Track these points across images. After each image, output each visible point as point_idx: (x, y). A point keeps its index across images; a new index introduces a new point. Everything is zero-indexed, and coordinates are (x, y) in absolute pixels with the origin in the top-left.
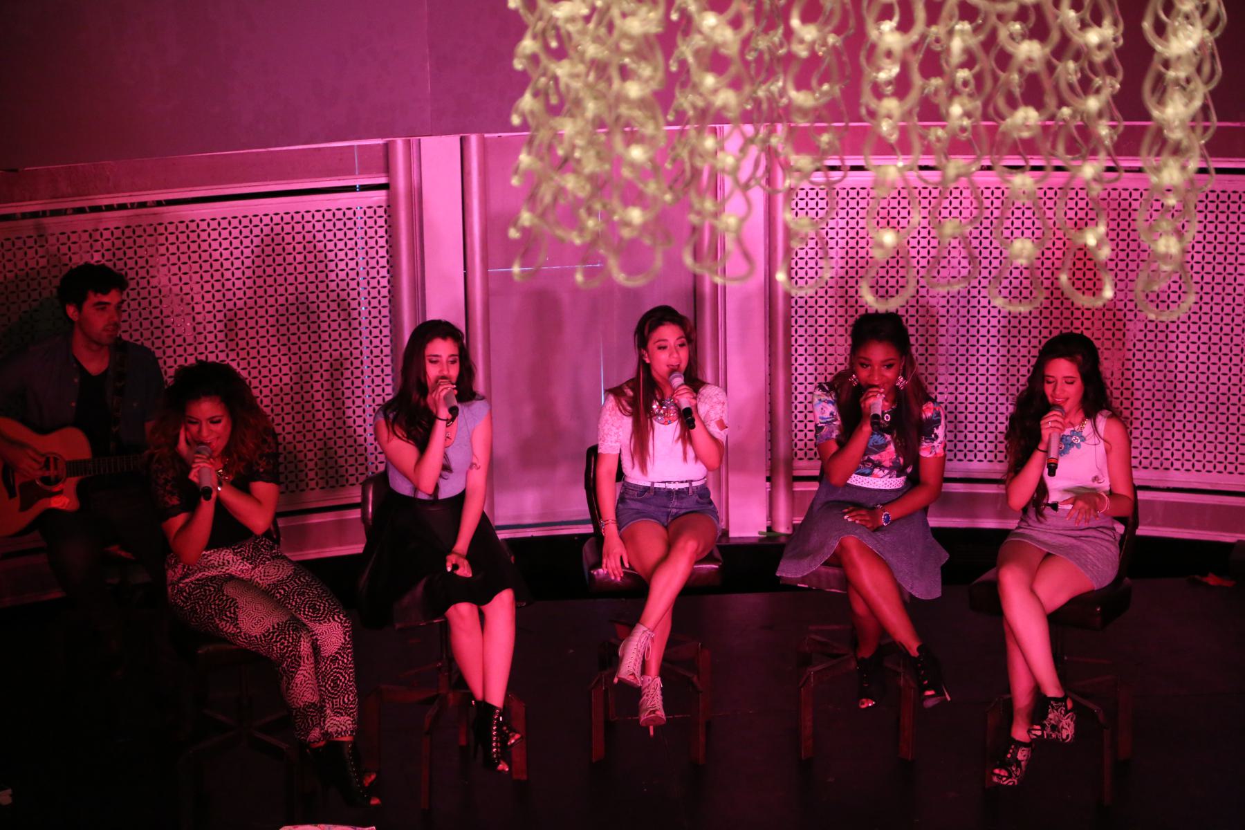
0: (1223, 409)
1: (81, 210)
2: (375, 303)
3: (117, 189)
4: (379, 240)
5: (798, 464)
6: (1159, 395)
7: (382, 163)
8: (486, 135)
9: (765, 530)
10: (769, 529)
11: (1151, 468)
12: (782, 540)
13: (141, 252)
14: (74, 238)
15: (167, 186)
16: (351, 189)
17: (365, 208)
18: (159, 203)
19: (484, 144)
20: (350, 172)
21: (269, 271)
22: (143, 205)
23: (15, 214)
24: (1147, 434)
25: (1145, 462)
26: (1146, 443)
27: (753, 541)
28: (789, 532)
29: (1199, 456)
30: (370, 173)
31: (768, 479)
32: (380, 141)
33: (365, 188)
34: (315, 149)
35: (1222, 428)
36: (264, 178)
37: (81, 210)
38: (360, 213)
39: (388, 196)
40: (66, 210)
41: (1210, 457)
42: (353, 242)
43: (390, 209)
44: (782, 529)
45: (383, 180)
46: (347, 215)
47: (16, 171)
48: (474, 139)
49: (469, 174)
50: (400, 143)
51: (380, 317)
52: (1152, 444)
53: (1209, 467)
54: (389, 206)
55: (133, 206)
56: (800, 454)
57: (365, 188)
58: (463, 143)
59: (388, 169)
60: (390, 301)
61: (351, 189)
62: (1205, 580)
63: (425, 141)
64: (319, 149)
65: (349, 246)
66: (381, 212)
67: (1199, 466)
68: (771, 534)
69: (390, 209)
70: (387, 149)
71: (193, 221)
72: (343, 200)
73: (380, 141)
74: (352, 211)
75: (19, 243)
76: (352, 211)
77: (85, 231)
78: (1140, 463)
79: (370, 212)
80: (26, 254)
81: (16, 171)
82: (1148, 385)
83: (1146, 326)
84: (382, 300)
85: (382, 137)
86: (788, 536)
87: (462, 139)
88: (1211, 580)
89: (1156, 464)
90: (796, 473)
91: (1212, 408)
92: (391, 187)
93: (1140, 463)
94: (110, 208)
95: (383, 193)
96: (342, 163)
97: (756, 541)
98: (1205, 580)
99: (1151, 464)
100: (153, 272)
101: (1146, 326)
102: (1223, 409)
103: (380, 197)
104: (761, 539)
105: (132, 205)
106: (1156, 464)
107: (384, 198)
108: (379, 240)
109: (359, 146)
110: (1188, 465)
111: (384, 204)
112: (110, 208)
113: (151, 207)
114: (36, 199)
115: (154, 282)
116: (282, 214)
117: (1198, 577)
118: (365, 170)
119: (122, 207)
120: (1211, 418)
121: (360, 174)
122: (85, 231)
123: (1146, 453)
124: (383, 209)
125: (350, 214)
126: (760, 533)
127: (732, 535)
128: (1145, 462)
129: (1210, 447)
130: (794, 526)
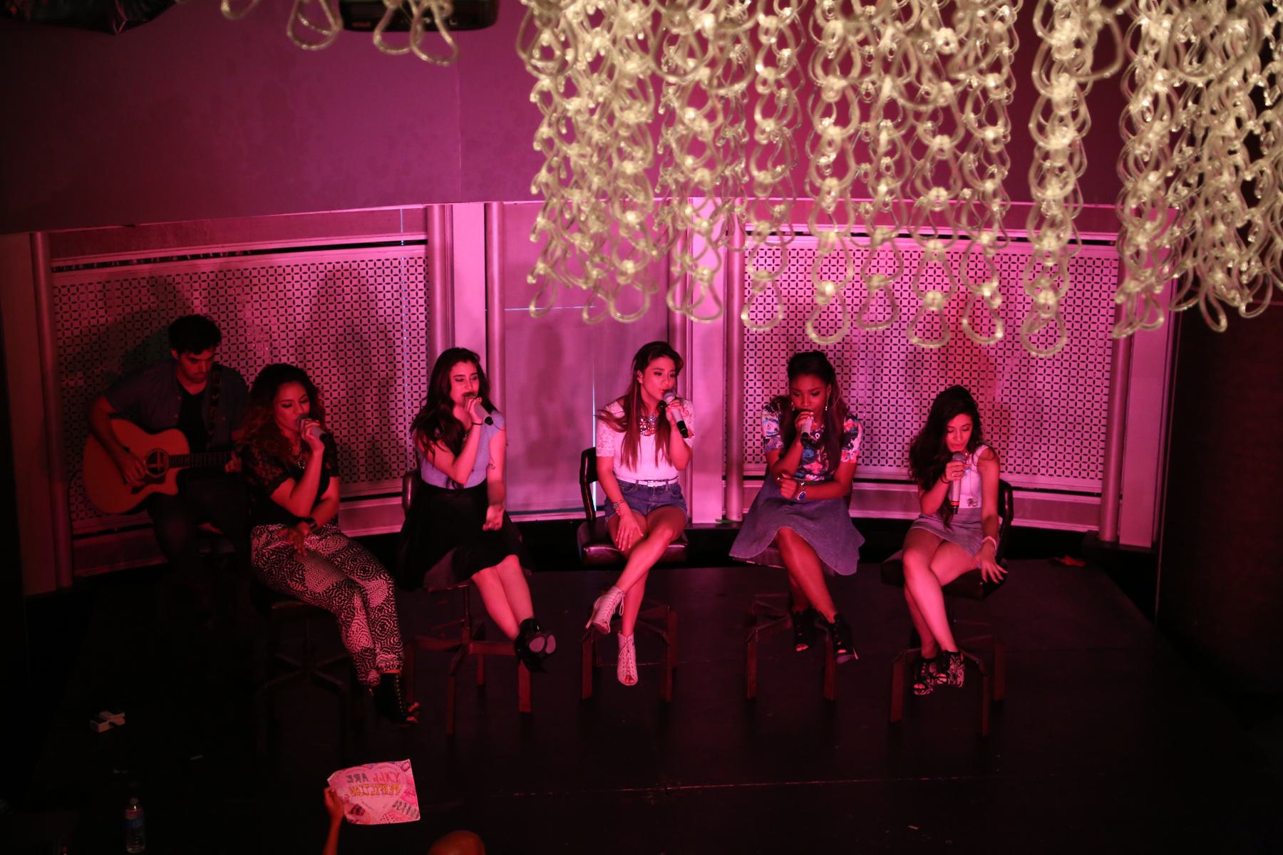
0: (1079, 427)
1: (184, 258)
2: (414, 334)
3: (212, 241)
5: (747, 466)
6: (1030, 416)
8: (505, 203)
9: (721, 518)
10: (724, 517)
11: (1023, 473)
12: (735, 526)
13: (231, 291)
16: (397, 243)
17: (408, 259)
18: (245, 253)
19: (503, 210)
20: (396, 230)
21: (332, 307)
22: (232, 254)
23: (131, 261)
24: (1020, 446)
25: (1019, 469)
26: (1019, 454)
27: (707, 527)
28: (740, 520)
29: (1060, 464)
30: (412, 231)
31: (724, 478)
32: (421, 206)
33: (408, 243)
35: (1078, 443)
36: (327, 234)
38: (404, 263)
39: (426, 249)
40: (172, 257)
41: (1068, 465)
42: (398, 285)
43: (428, 260)
44: (734, 517)
45: (422, 237)
46: (393, 263)
47: (133, 226)
48: (495, 206)
49: (491, 232)
50: (436, 207)
51: (418, 345)
52: (1024, 454)
53: (1068, 473)
54: (427, 258)
55: (225, 255)
56: (750, 458)
57: (408, 243)
58: (487, 208)
59: (426, 228)
60: (426, 332)
61: (397, 243)
62: (1062, 561)
63: (454, 205)
65: (395, 289)
66: (420, 262)
67: (1059, 472)
68: (726, 522)
69: (428, 260)
70: (426, 213)
72: (391, 252)
73: (421, 206)
75: (134, 283)
77: (187, 274)
78: (1015, 469)
79: (412, 262)
80: (140, 292)
81: (133, 226)
82: (1022, 408)
84: (420, 332)
85: (422, 203)
86: (740, 524)
87: (485, 205)
88: (1068, 561)
89: (1027, 470)
90: (746, 474)
91: (1070, 427)
92: (429, 241)
93: (1015, 469)
94: (206, 256)
96: (390, 224)
97: (713, 527)
98: (1062, 561)
99: (1023, 470)
100: (239, 307)
102: (1079, 427)
103: (420, 250)
104: (717, 525)
106: (1027, 470)
107: (423, 251)
109: (404, 210)
110: (1051, 471)
111: (423, 256)
112: (206, 256)
113: (239, 255)
115: (240, 315)
116: (342, 262)
117: (1057, 559)
118: (409, 229)
119: (216, 255)
120: (1070, 435)
121: (405, 231)
122: (187, 274)
123: (1019, 461)
124: (422, 260)
125: (395, 263)
126: (717, 520)
127: (694, 522)
128: (1019, 469)
129: (1069, 458)
130: (744, 516)
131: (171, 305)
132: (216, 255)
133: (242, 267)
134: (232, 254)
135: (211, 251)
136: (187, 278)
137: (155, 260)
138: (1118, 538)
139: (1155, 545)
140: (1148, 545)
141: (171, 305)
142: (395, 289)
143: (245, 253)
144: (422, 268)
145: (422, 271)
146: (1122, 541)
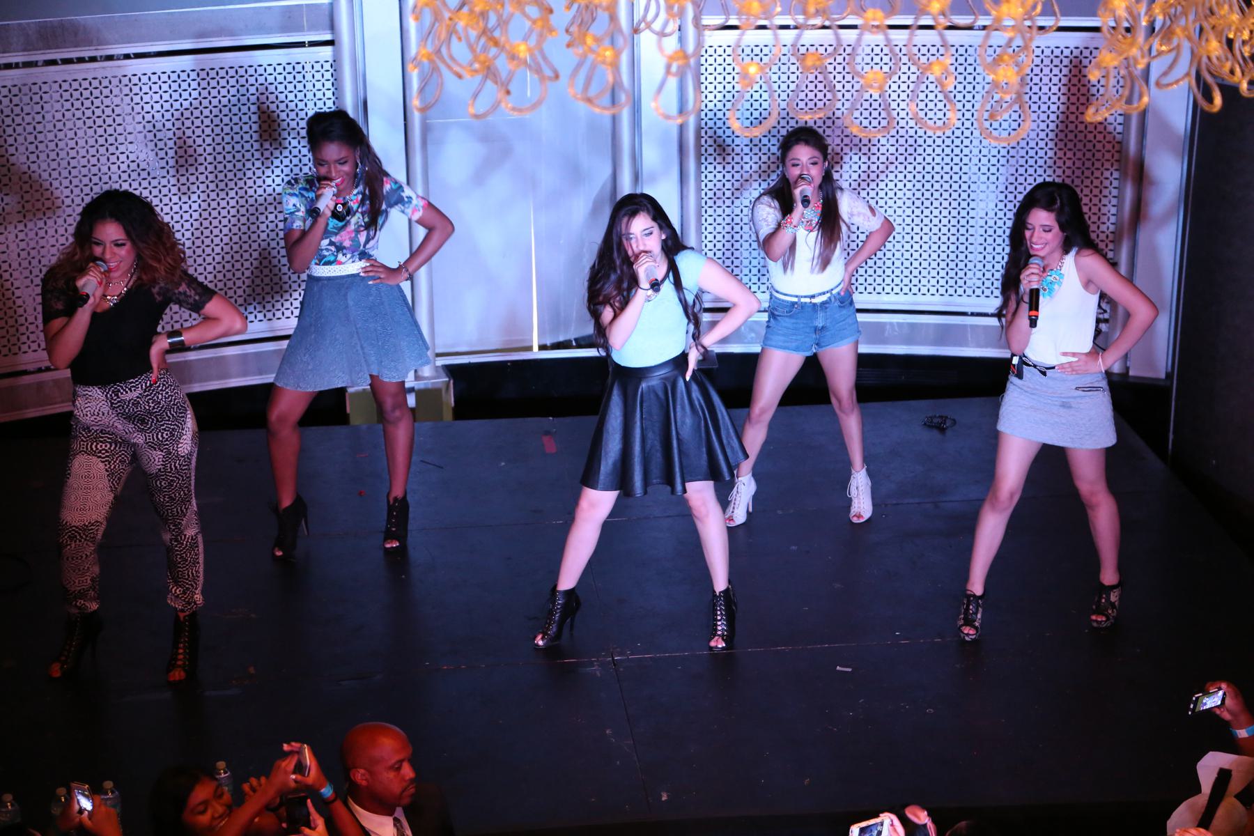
1: (53, 62)
3: (89, 43)
4: (326, 92)
7: (327, 21)
14: (45, 88)
15: (129, 41)
18: (127, 57)
20: (299, 29)
22: (110, 58)
30: (318, 30)
34: (266, 7)
37: (53, 62)
42: (302, 94)
43: (336, 64)
45: (328, 37)
46: (296, 68)
49: (408, 31)
59: (332, 27)
64: (269, 8)
65: (299, 98)
66: (327, 66)
69: (336, 64)
71: (154, 73)
74: (301, 66)
76: (301, 66)
79: (317, 67)
83: (1017, 170)
94: (81, 60)
95: (329, 49)
101: (1017, 170)
103: (327, 52)
105: (101, 57)
108: (326, 92)
111: (331, 61)
112: (81, 60)
113: (119, 59)
114: (9, 52)
118: (313, 27)
121: (309, 30)
124: (329, 64)
125: (299, 68)
131: (39, 118)
132: (93, 59)
133: (120, 73)
134: (110, 58)
135: (86, 54)
136: (56, 86)
137: (17, 66)
138: (1127, 369)
139: (1169, 376)
140: (1163, 376)
141: (39, 118)
142: (299, 98)
143: (127, 57)
144: (329, 73)
145: (330, 77)
146: (1131, 373)
